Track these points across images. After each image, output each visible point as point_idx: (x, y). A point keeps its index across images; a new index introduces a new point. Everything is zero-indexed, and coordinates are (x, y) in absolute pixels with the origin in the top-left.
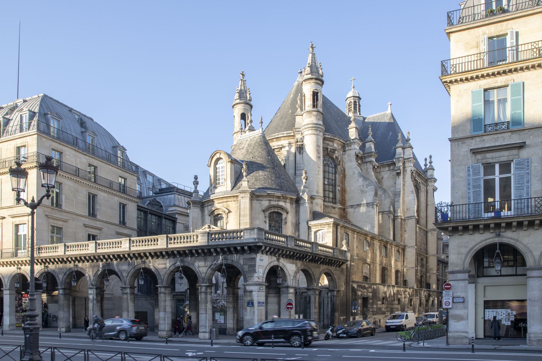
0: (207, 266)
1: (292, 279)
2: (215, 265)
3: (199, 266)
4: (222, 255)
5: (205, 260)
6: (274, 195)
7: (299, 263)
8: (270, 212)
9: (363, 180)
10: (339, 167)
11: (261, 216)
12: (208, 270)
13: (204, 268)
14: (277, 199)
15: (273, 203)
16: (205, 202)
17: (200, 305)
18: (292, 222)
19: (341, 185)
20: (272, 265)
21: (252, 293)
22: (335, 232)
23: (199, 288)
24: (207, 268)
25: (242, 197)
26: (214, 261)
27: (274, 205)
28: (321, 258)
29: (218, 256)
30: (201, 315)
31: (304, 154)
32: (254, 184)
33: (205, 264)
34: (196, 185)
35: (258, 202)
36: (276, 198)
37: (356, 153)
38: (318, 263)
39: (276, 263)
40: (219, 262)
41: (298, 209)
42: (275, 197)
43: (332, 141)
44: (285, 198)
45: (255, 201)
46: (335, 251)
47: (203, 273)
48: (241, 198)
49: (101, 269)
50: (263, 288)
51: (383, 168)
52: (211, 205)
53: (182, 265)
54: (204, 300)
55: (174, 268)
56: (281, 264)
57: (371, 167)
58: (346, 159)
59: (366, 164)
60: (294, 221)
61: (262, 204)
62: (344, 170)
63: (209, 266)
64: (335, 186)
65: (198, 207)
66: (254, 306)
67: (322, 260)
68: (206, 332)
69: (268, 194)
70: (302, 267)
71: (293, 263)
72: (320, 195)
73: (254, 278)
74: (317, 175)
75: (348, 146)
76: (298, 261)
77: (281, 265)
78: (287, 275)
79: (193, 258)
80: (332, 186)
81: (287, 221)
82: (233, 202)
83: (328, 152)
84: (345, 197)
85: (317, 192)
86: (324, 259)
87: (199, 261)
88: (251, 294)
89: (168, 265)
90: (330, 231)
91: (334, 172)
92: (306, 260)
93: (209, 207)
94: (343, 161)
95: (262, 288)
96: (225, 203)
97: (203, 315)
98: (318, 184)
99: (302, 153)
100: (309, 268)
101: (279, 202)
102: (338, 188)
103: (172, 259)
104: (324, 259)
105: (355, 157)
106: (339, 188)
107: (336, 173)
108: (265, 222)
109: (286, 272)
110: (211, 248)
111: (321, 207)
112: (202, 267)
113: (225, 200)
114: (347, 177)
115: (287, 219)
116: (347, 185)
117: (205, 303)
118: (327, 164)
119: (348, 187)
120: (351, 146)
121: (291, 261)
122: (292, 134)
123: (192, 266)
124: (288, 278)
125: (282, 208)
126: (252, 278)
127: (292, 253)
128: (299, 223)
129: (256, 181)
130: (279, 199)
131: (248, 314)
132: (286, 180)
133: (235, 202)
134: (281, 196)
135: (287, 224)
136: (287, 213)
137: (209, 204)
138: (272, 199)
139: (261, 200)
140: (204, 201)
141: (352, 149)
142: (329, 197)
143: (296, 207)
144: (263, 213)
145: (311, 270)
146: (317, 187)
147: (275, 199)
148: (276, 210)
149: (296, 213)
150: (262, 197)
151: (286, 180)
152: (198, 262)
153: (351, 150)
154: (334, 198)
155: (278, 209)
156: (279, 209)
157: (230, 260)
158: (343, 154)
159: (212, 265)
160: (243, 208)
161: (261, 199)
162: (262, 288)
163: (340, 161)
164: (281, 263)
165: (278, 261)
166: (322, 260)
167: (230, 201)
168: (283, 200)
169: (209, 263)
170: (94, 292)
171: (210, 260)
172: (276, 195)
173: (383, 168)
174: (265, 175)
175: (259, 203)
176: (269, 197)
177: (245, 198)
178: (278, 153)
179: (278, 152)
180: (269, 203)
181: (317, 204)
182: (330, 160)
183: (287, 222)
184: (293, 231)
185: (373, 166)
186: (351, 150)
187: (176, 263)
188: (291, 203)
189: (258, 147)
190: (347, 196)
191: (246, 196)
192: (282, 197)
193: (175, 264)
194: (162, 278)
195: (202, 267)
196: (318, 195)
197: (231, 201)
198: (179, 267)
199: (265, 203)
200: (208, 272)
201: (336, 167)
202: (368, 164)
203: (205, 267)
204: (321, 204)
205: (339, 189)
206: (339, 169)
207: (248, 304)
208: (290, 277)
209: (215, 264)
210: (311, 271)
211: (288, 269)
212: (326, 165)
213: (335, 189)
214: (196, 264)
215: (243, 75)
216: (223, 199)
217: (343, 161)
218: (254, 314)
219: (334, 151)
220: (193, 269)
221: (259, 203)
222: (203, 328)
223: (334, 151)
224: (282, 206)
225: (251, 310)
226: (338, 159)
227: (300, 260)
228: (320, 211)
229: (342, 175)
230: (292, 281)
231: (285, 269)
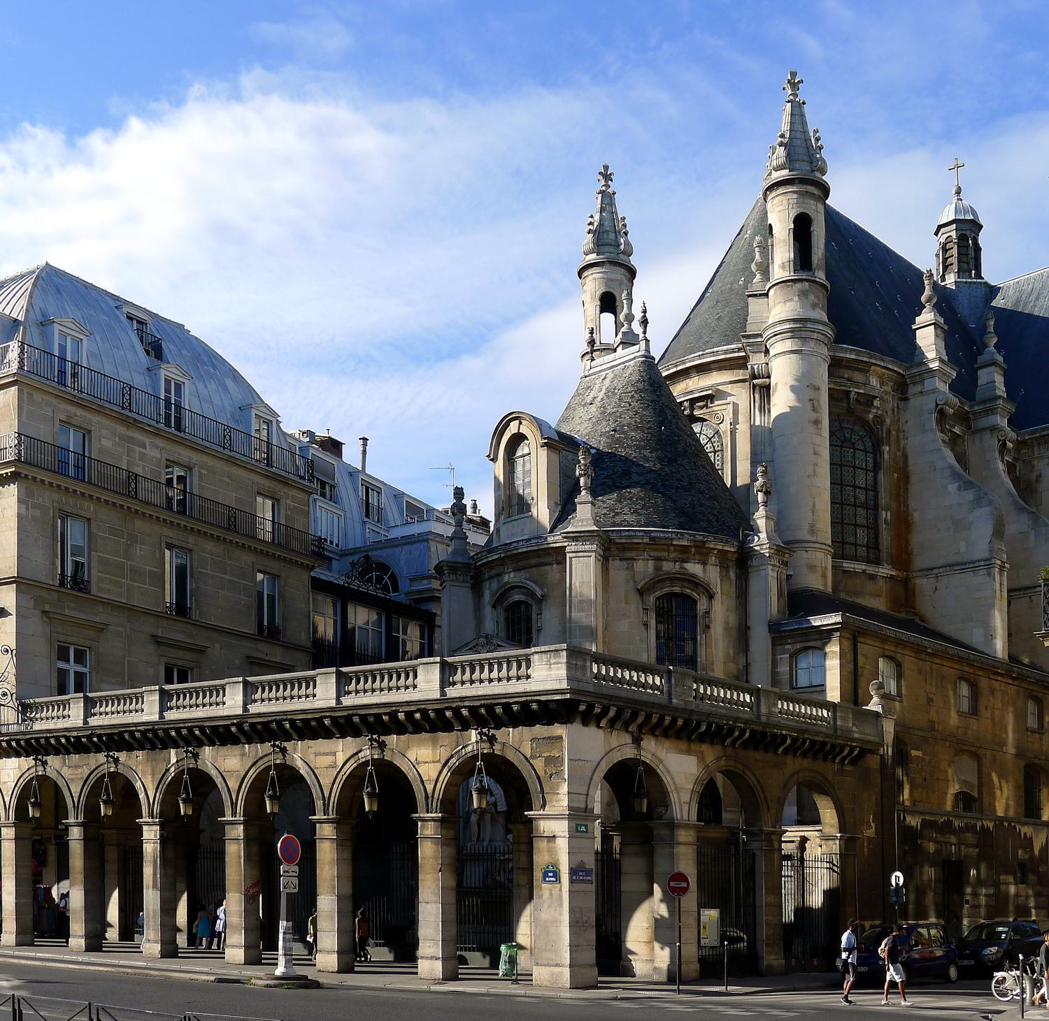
0: (439, 761)
1: (688, 800)
3: (418, 759)
5: (435, 743)
7: (710, 753)
8: (658, 593)
9: (959, 489)
10: (887, 448)
11: (633, 607)
14: (680, 556)
15: (667, 566)
18: (727, 623)
19: (894, 505)
20: (617, 757)
21: (555, 842)
22: (850, 656)
23: (419, 823)
24: (439, 766)
27: (669, 573)
28: (784, 738)
32: (613, 510)
33: (434, 755)
34: (459, 516)
35: (625, 563)
38: (775, 753)
39: (629, 752)
40: (469, 748)
41: (744, 583)
42: (672, 548)
43: (860, 370)
44: (702, 554)
45: (617, 562)
46: (838, 714)
49: (172, 769)
50: (586, 826)
51: (1039, 444)
53: (376, 757)
55: (355, 765)
56: (649, 756)
57: (996, 445)
58: (909, 424)
59: (978, 436)
60: (733, 620)
62: (905, 457)
64: (876, 508)
66: (560, 882)
67: (789, 741)
69: (652, 539)
70: (723, 762)
71: (689, 752)
72: (820, 540)
73: (559, 796)
74: (809, 476)
76: (705, 748)
77: (646, 757)
78: (670, 788)
80: (867, 508)
81: (710, 621)
83: (848, 404)
84: (907, 542)
85: (812, 531)
86: (794, 740)
87: (420, 744)
88: (552, 845)
89: (341, 758)
90: (834, 652)
91: (870, 466)
92: (734, 742)
94: (898, 431)
95: (583, 828)
96: (534, 569)
98: (814, 506)
100: (746, 766)
101: (685, 565)
102: (885, 515)
104: (794, 740)
105: (934, 416)
106: (889, 514)
107: (877, 468)
108: (646, 625)
109: (666, 779)
111: (824, 576)
113: (533, 561)
114: (914, 479)
115: (712, 615)
116: (912, 503)
118: (850, 441)
119: (916, 510)
121: (684, 745)
124: (674, 797)
125: (694, 582)
126: (555, 797)
127: (680, 722)
128: (749, 628)
129: (620, 502)
130: (685, 556)
131: (545, 905)
132: (710, 497)
134: (690, 546)
135: (712, 630)
136: (711, 597)
138: (666, 554)
139: (634, 559)
142: (856, 545)
143: (739, 577)
144: (637, 597)
145: (753, 774)
146: (810, 513)
148: (677, 589)
149: (738, 597)
150: (637, 549)
151: (710, 497)
154: (874, 545)
155: (682, 587)
156: (686, 584)
158: (898, 407)
159: (452, 756)
160: (577, 584)
161: (633, 554)
162: (583, 828)
163: (889, 432)
164: (647, 751)
165: (639, 747)
166: (789, 741)
168: (697, 557)
169: (445, 754)
170: (156, 836)
173: (1039, 444)
175: (627, 568)
176: (656, 550)
178: (702, 412)
179: (704, 410)
181: (812, 568)
182: (856, 428)
183: (712, 626)
184: (731, 653)
185: (999, 441)
187: (360, 751)
188: (724, 567)
190: (916, 539)
192: (693, 550)
195: (427, 762)
196: (813, 539)
197: (551, 564)
198: (366, 763)
199: (645, 567)
200: (441, 779)
201: (877, 450)
202: (987, 435)
203: (433, 762)
204: (826, 568)
205: (889, 518)
206: (886, 456)
207: (545, 875)
208: (678, 793)
210: (752, 778)
211: (671, 770)
212: (845, 444)
213: (876, 520)
214: (412, 755)
215: (607, 177)
217: (898, 431)
218: (561, 905)
219: (868, 400)
221: (627, 568)
223: (868, 400)
224: (693, 576)
225: (553, 892)
226: (882, 426)
227: (712, 743)
228: (821, 588)
229: (896, 475)
230: (685, 807)
231: (660, 770)
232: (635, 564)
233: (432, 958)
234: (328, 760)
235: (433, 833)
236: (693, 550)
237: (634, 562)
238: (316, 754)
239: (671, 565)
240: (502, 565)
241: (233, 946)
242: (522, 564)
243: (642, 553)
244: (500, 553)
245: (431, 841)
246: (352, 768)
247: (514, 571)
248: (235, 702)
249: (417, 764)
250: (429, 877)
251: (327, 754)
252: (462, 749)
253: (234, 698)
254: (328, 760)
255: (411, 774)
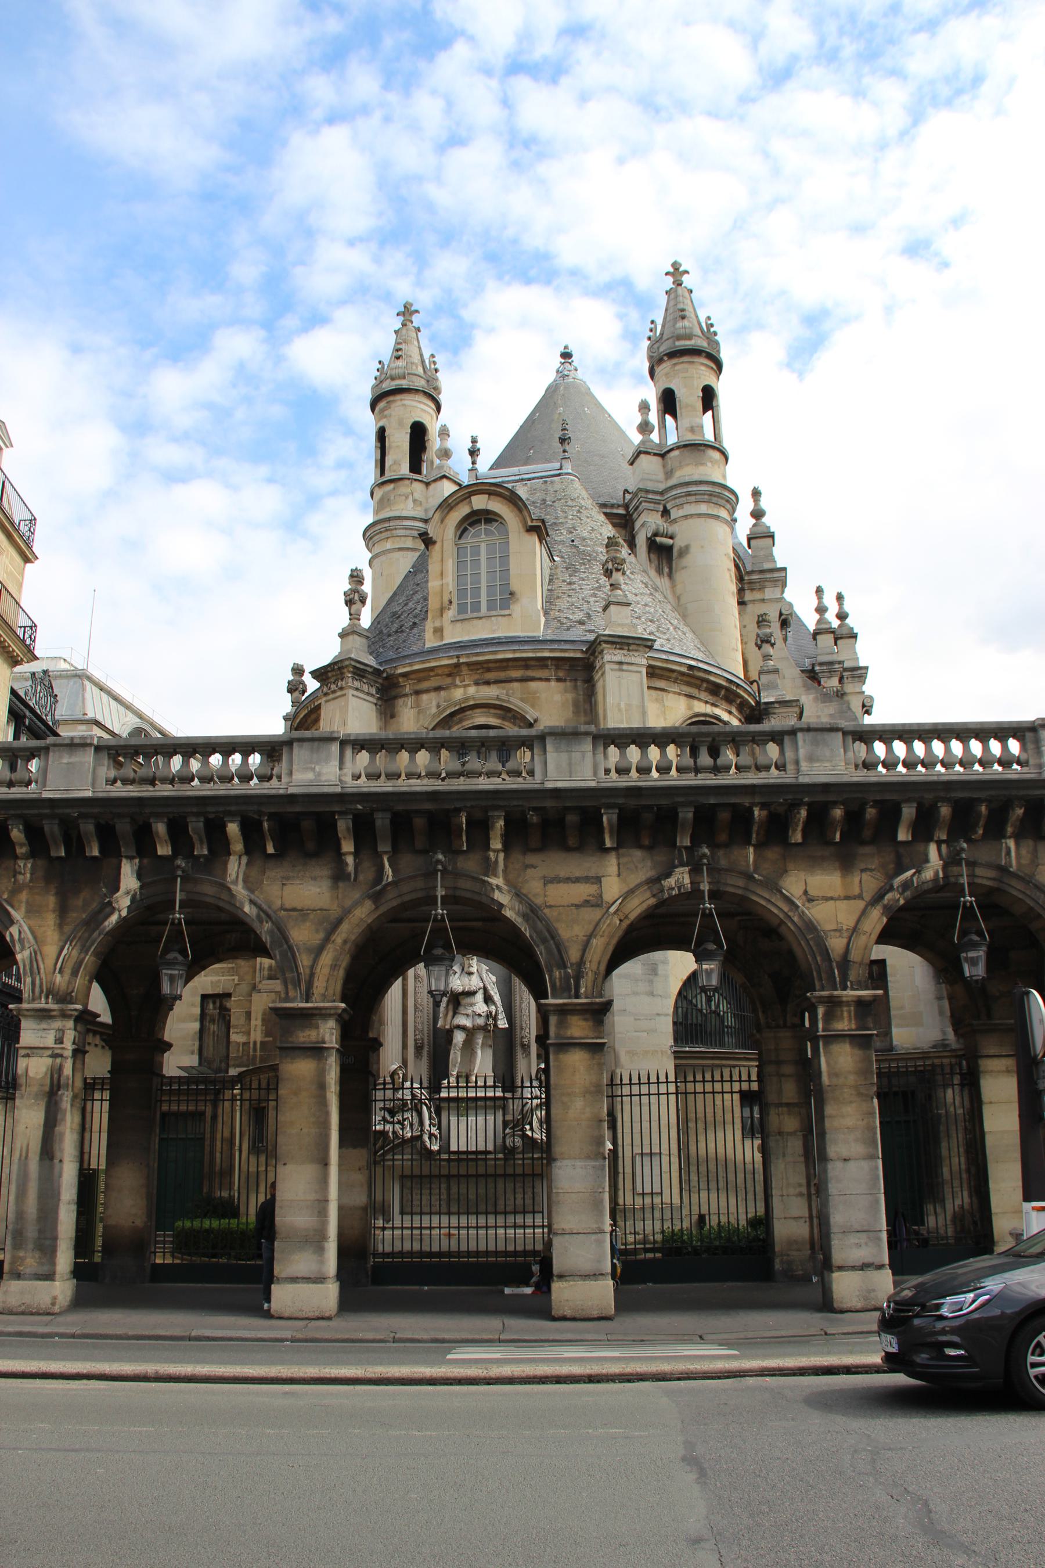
0: (860, 897)
2: (904, 891)
3: (812, 892)
4: (939, 843)
5: (846, 863)
6: (707, 676)
9: (816, 700)
12: (864, 913)
13: (843, 905)
15: (700, 707)
16: (405, 675)
17: (829, 1110)
23: (821, 1011)
24: (861, 905)
25: (621, 663)
26: (900, 869)
29: (920, 847)
30: (839, 1165)
31: (679, 576)
36: (707, 690)
37: (781, 614)
40: (928, 874)
42: (705, 685)
47: (840, 930)
48: (616, 667)
52: (438, 689)
54: (851, 1079)
55: (652, 901)
61: (666, 704)
63: (868, 896)
65: (368, 694)
68: (881, 1267)
74: (733, 649)
75: (752, 590)
79: (773, 853)
82: (553, 683)
89: (612, 888)
93: (425, 697)
96: (516, 685)
97: (852, 1164)
99: (670, 575)
103: (638, 854)
110: (908, 800)
112: (828, 899)
117: (860, 1094)
120: (762, 589)
122: (621, 511)
123: (766, 895)
133: (559, 684)
137: (425, 685)
140: (400, 671)
141: (771, 600)
147: (704, 695)
150: (667, 679)
152: (802, 875)
153: (763, 600)
157: (989, 866)
159: (891, 889)
167: (540, 679)
169: (868, 882)
171: (874, 863)
172: (712, 678)
174: (646, 605)
176: (689, 684)
177: (630, 668)
180: (690, 708)
186: (763, 600)
187: (668, 875)
189: (579, 512)
191: (633, 660)
193: (655, 881)
194: (574, 955)
195: (832, 898)
197: (548, 680)
203: (847, 898)
209: (906, 885)
216: (504, 669)
220: (777, 908)
221: (657, 700)
222: (858, 1245)
232: (665, 698)
233: (864, 1267)
234: (584, 891)
235: (853, 1026)
236: (723, 692)
237: (664, 694)
238: (548, 881)
239: (702, 705)
240: (449, 675)
241: (294, 1280)
242: (491, 676)
243: (672, 684)
244: (458, 657)
245: (851, 1043)
246: (645, 906)
247: (477, 684)
248: (319, 774)
249: (810, 900)
250: (849, 1109)
251: (586, 880)
252: (915, 873)
253: (313, 769)
254: (584, 891)
255: (796, 919)
